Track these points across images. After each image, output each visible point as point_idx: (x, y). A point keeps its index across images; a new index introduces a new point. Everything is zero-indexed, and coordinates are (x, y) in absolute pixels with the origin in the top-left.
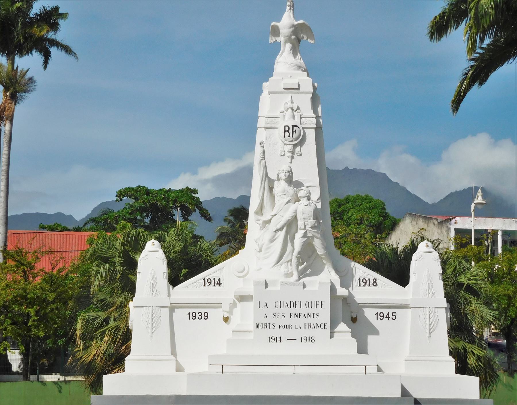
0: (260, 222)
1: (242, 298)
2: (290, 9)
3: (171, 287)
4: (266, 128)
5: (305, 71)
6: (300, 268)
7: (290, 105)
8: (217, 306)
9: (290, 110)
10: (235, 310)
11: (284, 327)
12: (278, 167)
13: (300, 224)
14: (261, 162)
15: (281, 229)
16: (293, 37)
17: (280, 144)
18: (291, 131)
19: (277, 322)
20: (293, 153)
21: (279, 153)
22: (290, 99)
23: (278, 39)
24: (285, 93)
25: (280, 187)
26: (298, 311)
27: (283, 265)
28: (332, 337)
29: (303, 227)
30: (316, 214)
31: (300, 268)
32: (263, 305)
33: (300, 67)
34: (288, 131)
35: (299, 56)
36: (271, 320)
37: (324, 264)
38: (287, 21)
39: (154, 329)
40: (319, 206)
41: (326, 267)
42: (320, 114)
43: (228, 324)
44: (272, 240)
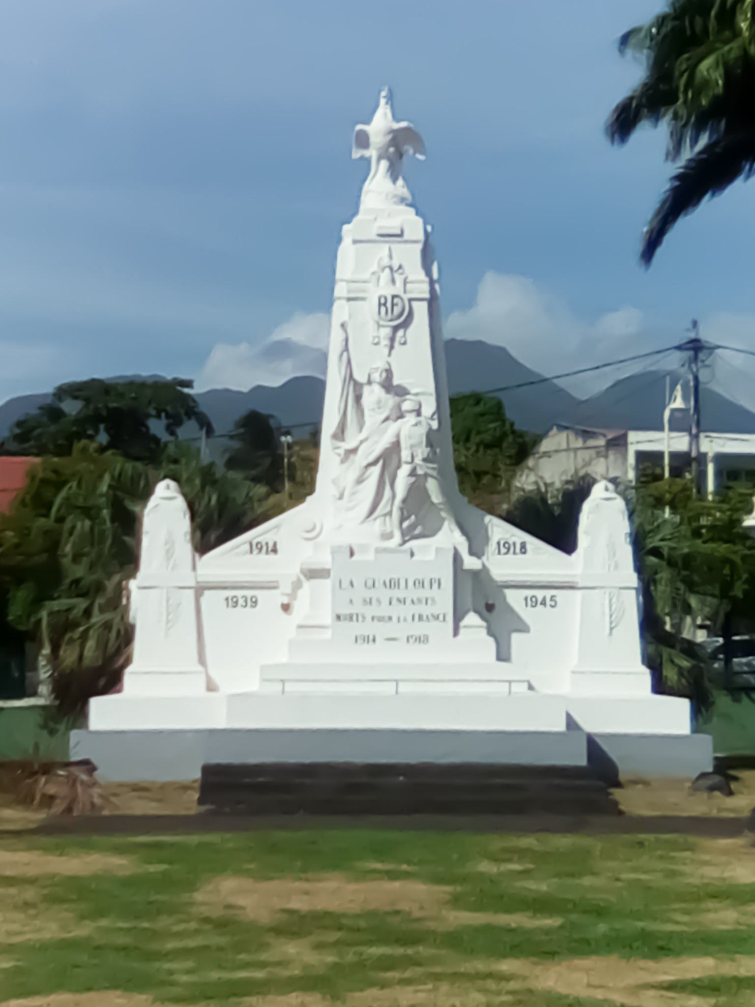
0: (341, 451)
1: (313, 574)
2: (387, 103)
3: (197, 556)
4: (349, 299)
5: (410, 205)
6: (406, 524)
7: (386, 261)
8: (271, 586)
9: (387, 271)
10: (300, 593)
11: (381, 619)
12: (369, 362)
13: (405, 455)
14: (341, 355)
15: (374, 463)
16: (392, 150)
17: (371, 326)
18: (389, 305)
19: (369, 611)
20: (392, 339)
21: (371, 339)
22: (387, 252)
23: (366, 153)
24: (379, 243)
25: (373, 395)
26: (400, 593)
27: (378, 521)
28: (456, 632)
29: (409, 459)
30: (431, 439)
31: (406, 524)
32: (346, 584)
33: (402, 200)
34: (385, 304)
35: (400, 182)
36: (358, 608)
37: (443, 520)
38: (381, 124)
39: (170, 624)
40: (435, 425)
41: (446, 524)
42: (435, 275)
43: (290, 614)
44: (360, 481)
